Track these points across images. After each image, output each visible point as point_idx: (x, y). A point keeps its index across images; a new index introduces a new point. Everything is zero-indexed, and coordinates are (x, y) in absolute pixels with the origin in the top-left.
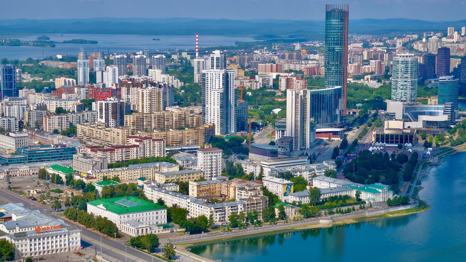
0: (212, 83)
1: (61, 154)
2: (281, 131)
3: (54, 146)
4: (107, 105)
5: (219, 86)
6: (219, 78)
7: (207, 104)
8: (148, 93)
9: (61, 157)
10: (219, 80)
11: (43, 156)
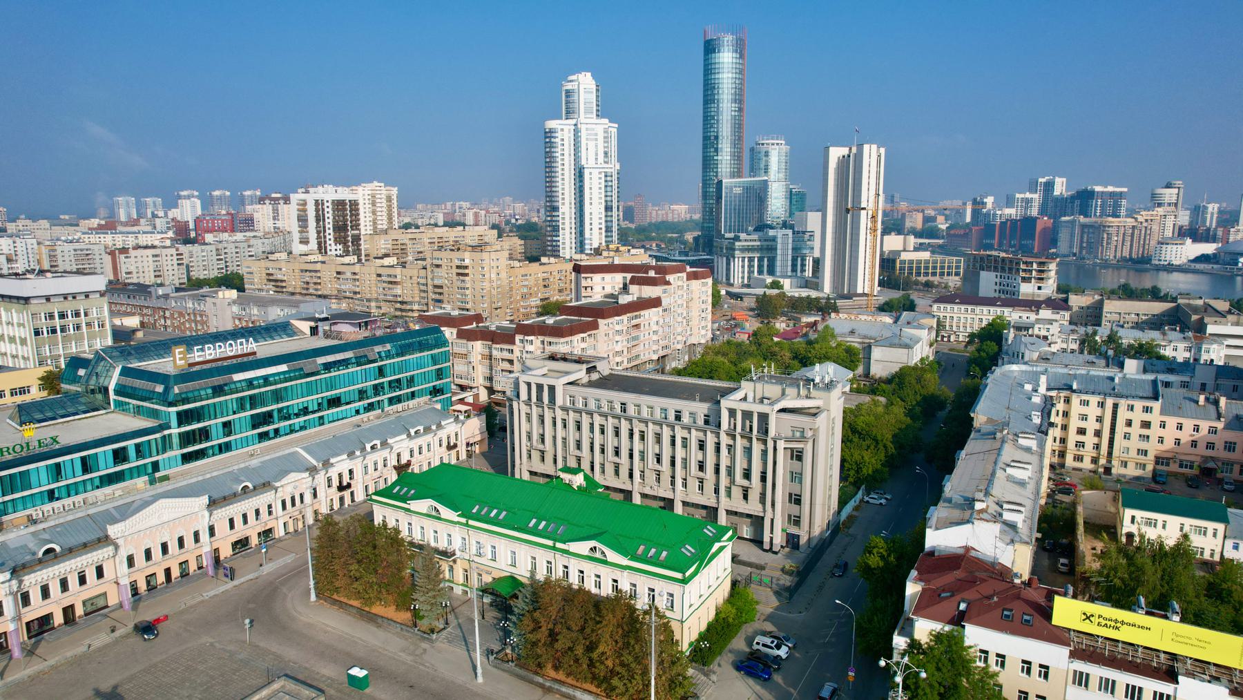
1: (381, 372)
2: (746, 260)
3: (314, 331)
5: (596, 159)
6: (596, 140)
7: (563, 204)
8: (367, 197)
9: (377, 389)
11: (278, 396)
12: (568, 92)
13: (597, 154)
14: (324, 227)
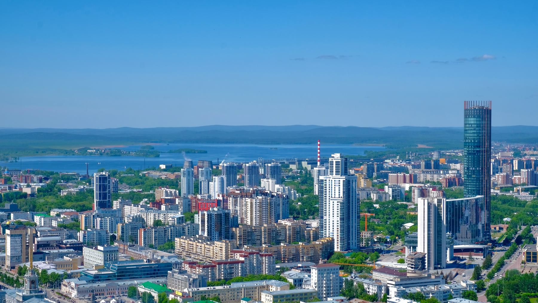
0: (330, 191)
2: (411, 247)
4: (210, 216)
5: (339, 195)
6: (339, 186)
7: (325, 215)
9: (154, 274)
10: (339, 188)
11: (133, 272)
12: (331, 162)
13: (339, 192)
14: (211, 225)
